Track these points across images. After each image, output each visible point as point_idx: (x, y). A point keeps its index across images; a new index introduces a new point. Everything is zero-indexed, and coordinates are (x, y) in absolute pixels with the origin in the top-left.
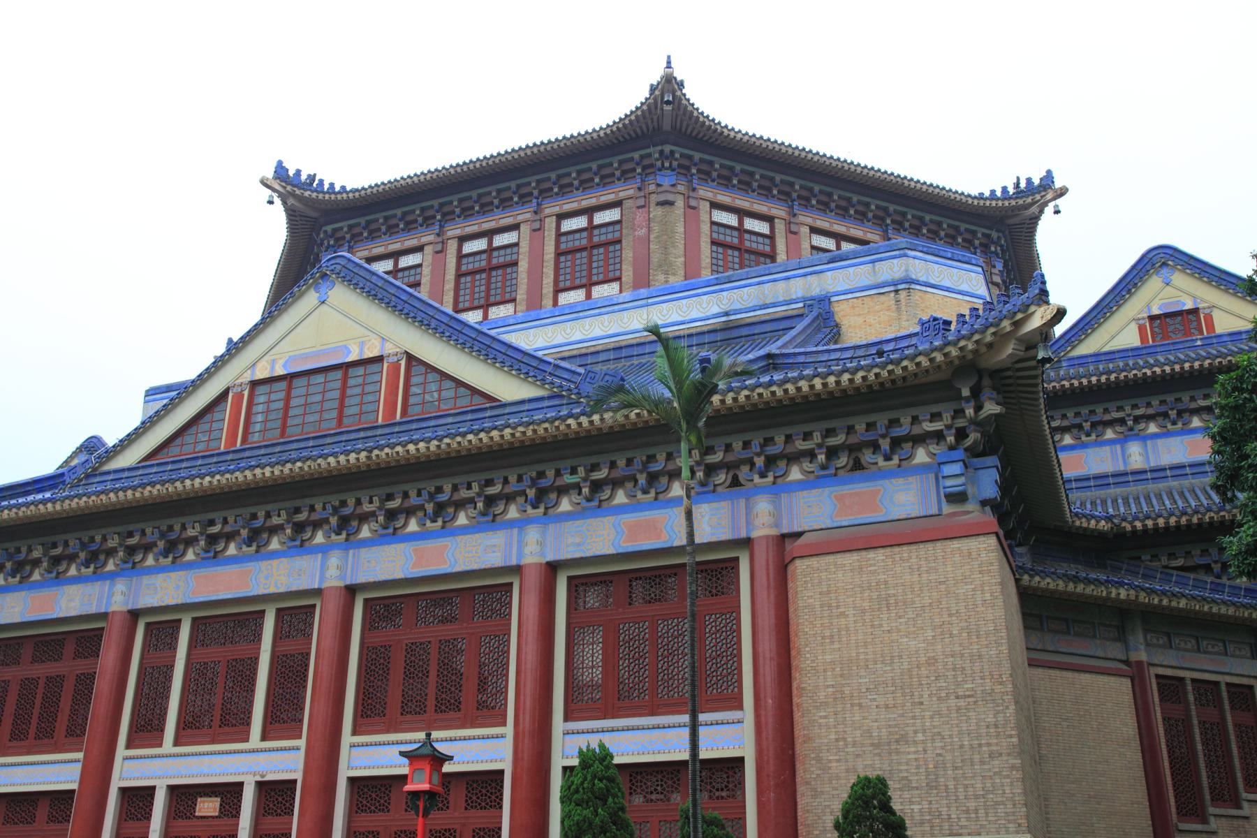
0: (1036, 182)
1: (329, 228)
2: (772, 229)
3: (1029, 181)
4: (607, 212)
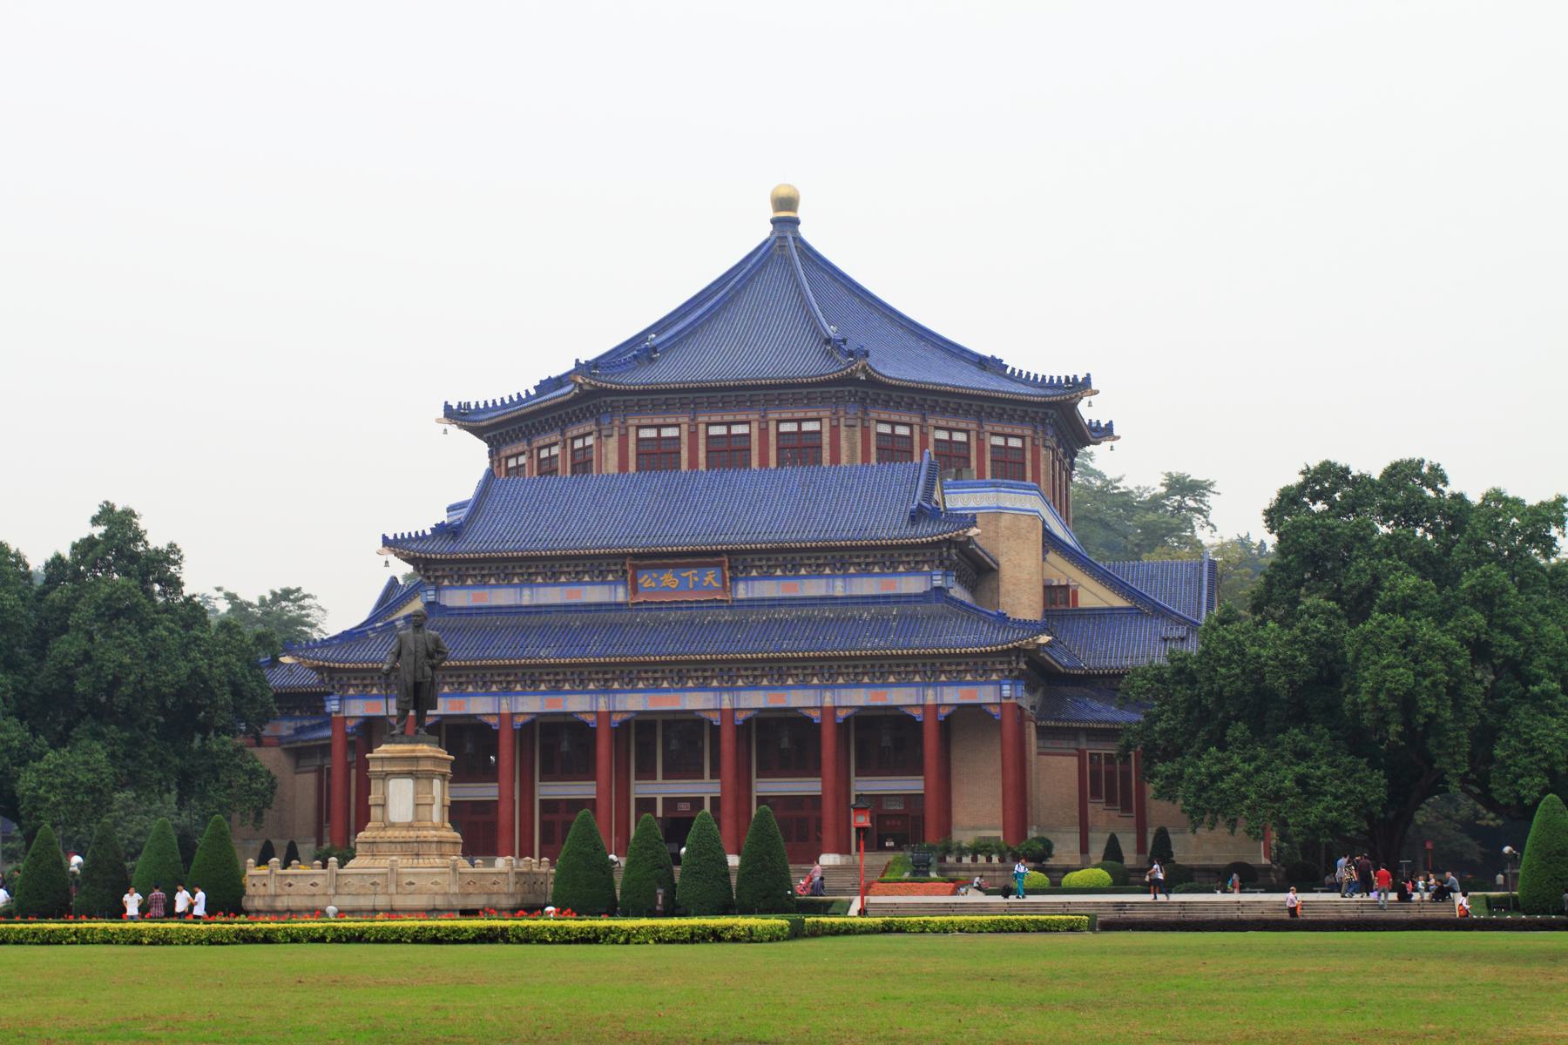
0: (1080, 380)
1: (608, 400)
2: (912, 432)
4: (811, 423)
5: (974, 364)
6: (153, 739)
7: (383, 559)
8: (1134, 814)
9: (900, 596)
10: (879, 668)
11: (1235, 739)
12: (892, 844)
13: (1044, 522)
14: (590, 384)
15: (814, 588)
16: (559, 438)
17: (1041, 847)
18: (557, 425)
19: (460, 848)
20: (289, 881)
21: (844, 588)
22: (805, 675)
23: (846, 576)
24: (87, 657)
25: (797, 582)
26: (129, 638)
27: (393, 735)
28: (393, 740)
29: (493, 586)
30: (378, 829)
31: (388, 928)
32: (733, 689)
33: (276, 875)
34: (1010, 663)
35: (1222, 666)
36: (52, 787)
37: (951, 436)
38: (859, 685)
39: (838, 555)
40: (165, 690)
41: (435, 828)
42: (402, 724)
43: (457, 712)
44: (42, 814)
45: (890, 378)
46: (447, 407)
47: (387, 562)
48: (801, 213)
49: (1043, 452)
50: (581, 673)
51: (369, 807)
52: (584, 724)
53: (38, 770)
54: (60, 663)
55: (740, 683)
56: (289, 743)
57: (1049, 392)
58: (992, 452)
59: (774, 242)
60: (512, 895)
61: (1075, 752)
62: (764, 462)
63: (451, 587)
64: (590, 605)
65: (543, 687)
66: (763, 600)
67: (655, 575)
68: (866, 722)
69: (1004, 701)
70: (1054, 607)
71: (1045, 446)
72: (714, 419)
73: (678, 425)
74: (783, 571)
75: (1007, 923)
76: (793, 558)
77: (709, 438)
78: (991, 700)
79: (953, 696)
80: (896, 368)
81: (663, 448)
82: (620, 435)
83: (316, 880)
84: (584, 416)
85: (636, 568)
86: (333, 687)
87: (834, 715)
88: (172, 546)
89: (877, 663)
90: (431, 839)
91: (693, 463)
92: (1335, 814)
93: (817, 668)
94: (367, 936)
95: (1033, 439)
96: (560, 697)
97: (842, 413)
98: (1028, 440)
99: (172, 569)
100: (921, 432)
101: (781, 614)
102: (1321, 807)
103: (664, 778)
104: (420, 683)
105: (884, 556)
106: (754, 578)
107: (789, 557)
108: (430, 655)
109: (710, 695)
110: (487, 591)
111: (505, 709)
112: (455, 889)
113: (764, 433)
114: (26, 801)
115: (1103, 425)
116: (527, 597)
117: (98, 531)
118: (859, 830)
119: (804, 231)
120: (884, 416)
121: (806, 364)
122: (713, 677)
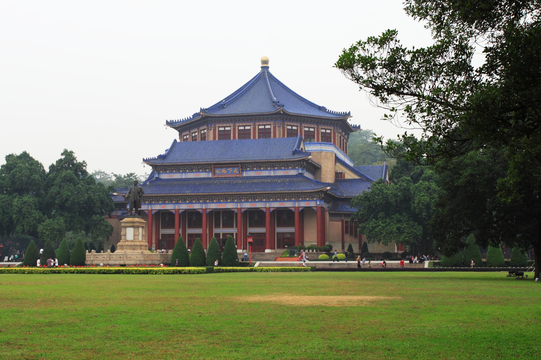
0: (347, 113)
1: (210, 119)
3: (346, 112)
5: (317, 108)
6: (78, 216)
7: (143, 165)
8: (358, 238)
9: (289, 176)
10: (282, 196)
11: (380, 217)
12: (287, 246)
13: (335, 154)
14: (204, 115)
15: (265, 173)
16: (197, 130)
17: (328, 247)
18: (197, 126)
19: (147, 248)
20: (97, 256)
21: (274, 173)
22: (261, 198)
23: (274, 170)
24: (59, 193)
26: (70, 188)
27: (128, 216)
28: (128, 217)
29: (174, 173)
30: (123, 242)
31: (91, 270)
32: (241, 202)
33: (93, 255)
34: (319, 195)
35: (377, 196)
36: (47, 230)
37: (309, 129)
38: (277, 201)
39: (272, 164)
40: (81, 202)
41: (140, 242)
42: (131, 212)
43: (163, 209)
44: (44, 237)
45: (290, 113)
46: (167, 122)
47: (144, 166)
48: (270, 65)
49: (337, 134)
50: (198, 198)
51: (121, 236)
52: (199, 212)
53: (43, 225)
54: (51, 195)
55: (243, 200)
56: (120, 217)
57: (338, 117)
58: (321, 134)
59: (261, 73)
60: (159, 261)
61: (340, 220)
62: (254, 137)
63: (163, 173)
64: (202, 178)
65: (187, 202)
66: (251, 177)
67: (220, 170)
68: (279, 212)
69: (317, 206)
70: (338, 179)
71: (337, 132)
72: (240, 125)
73: (230, 127)
74: (256, 169)
75: (285, 269)
76: (259, 165)
77: (239, 130)
78: (314, 205)
79: (303, 204)
80: (292, 109)
81: (226, 133)
82: (214, 130)
83: (104, 256)
84: (204, 124)
85: (214, 168)
87: (270, 209)
88: (84, 161)
89: (282, 195)
90: (138, 245)
91: (234, 137)
92: (407, 238)
93: (265, 196)
94: (86, 272)
95: (334, 130)
96: (192, 204)
97: (277, 123)
98: (332, 131)
99: (84, 168)
100: (300, 128)
101: (255, 181)
102: (403, 236)
103: (223, 227)
104: (136, 201)
105: (286, 164)
106: (248, 171)
107: (258, 164)
108: (139, 193)
109: (234, 204)
110: (173, 174)
112: (142, 259)
113: (254, 128)
114: (40, 233)
115: (357, 126)
116: (184, 176)
117: (63, 157)
118: (249, 243)
119: (271, 70)
120: (289, 124)
121: (267, 108)
122: (235, 199)
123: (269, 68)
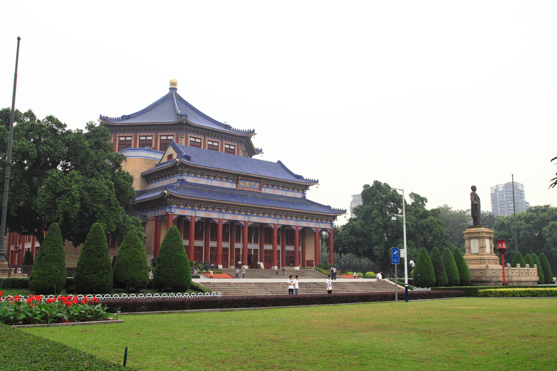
1: (185, 127)
9: (297, 198)
23: (285, 191)
25: (274, 190)
29: (199, 177)
38: (304, 221)
46: (101, 116)
48: (177, 87)
66: (268, 194)
82: (186, 138)
85: (241, 179)
86: (171, 204)
110: (199, 179)
111: (221, 217)
119: (178, 92)
123: (177, 90)
